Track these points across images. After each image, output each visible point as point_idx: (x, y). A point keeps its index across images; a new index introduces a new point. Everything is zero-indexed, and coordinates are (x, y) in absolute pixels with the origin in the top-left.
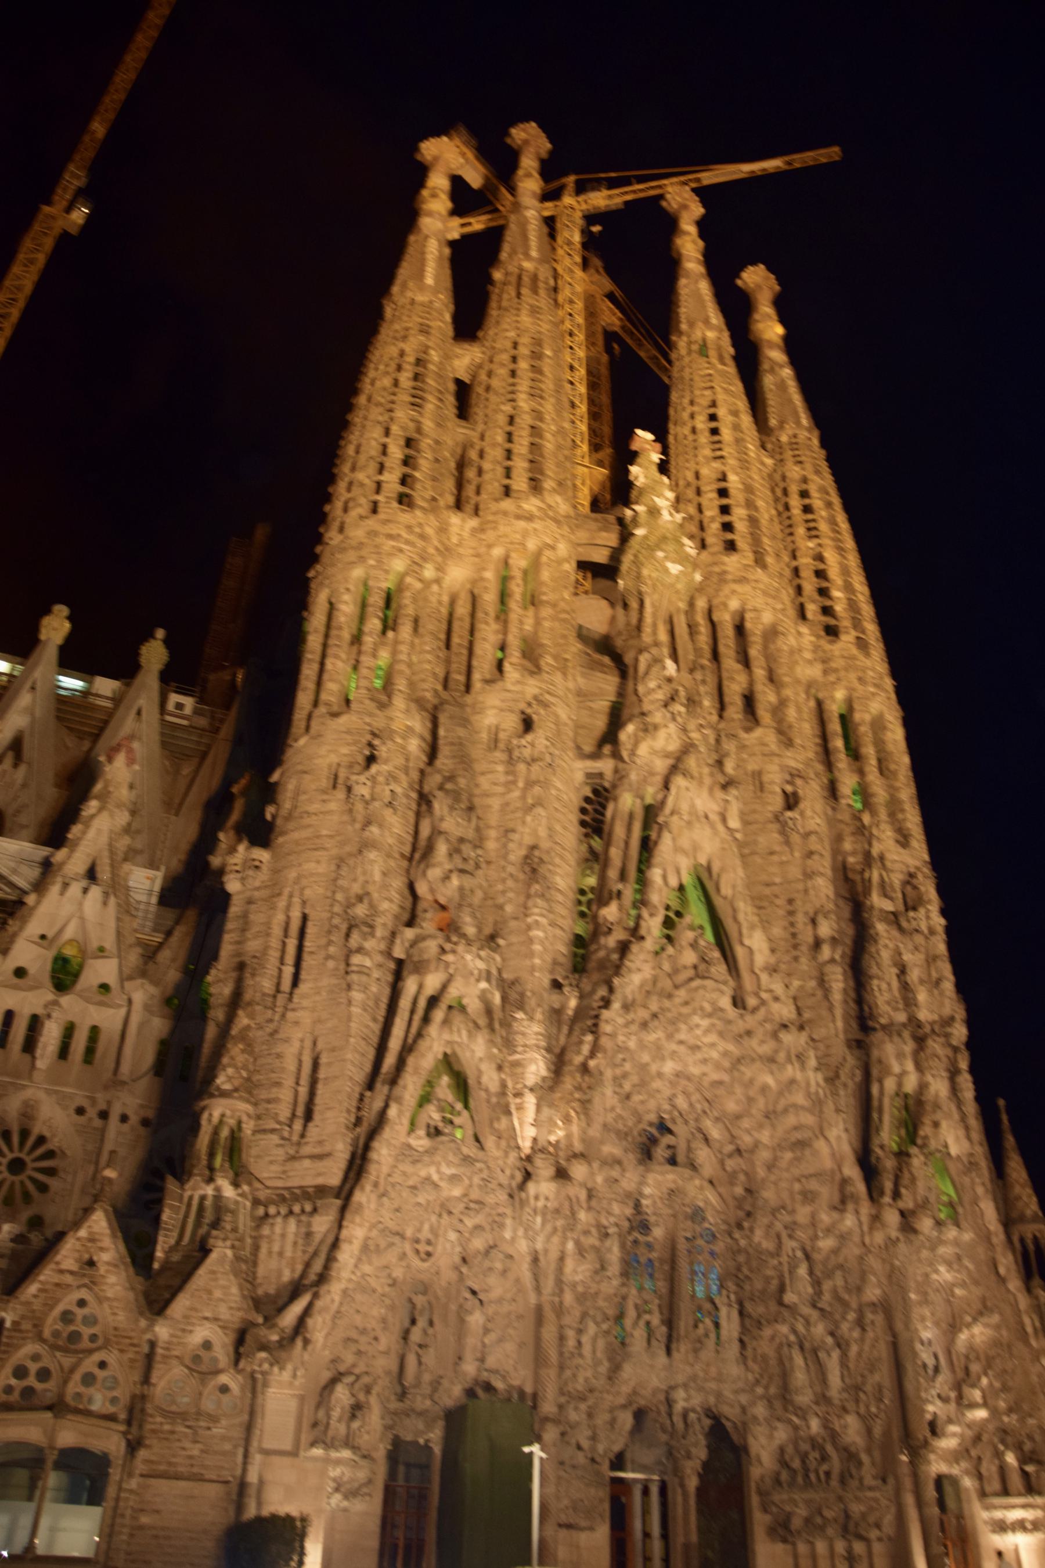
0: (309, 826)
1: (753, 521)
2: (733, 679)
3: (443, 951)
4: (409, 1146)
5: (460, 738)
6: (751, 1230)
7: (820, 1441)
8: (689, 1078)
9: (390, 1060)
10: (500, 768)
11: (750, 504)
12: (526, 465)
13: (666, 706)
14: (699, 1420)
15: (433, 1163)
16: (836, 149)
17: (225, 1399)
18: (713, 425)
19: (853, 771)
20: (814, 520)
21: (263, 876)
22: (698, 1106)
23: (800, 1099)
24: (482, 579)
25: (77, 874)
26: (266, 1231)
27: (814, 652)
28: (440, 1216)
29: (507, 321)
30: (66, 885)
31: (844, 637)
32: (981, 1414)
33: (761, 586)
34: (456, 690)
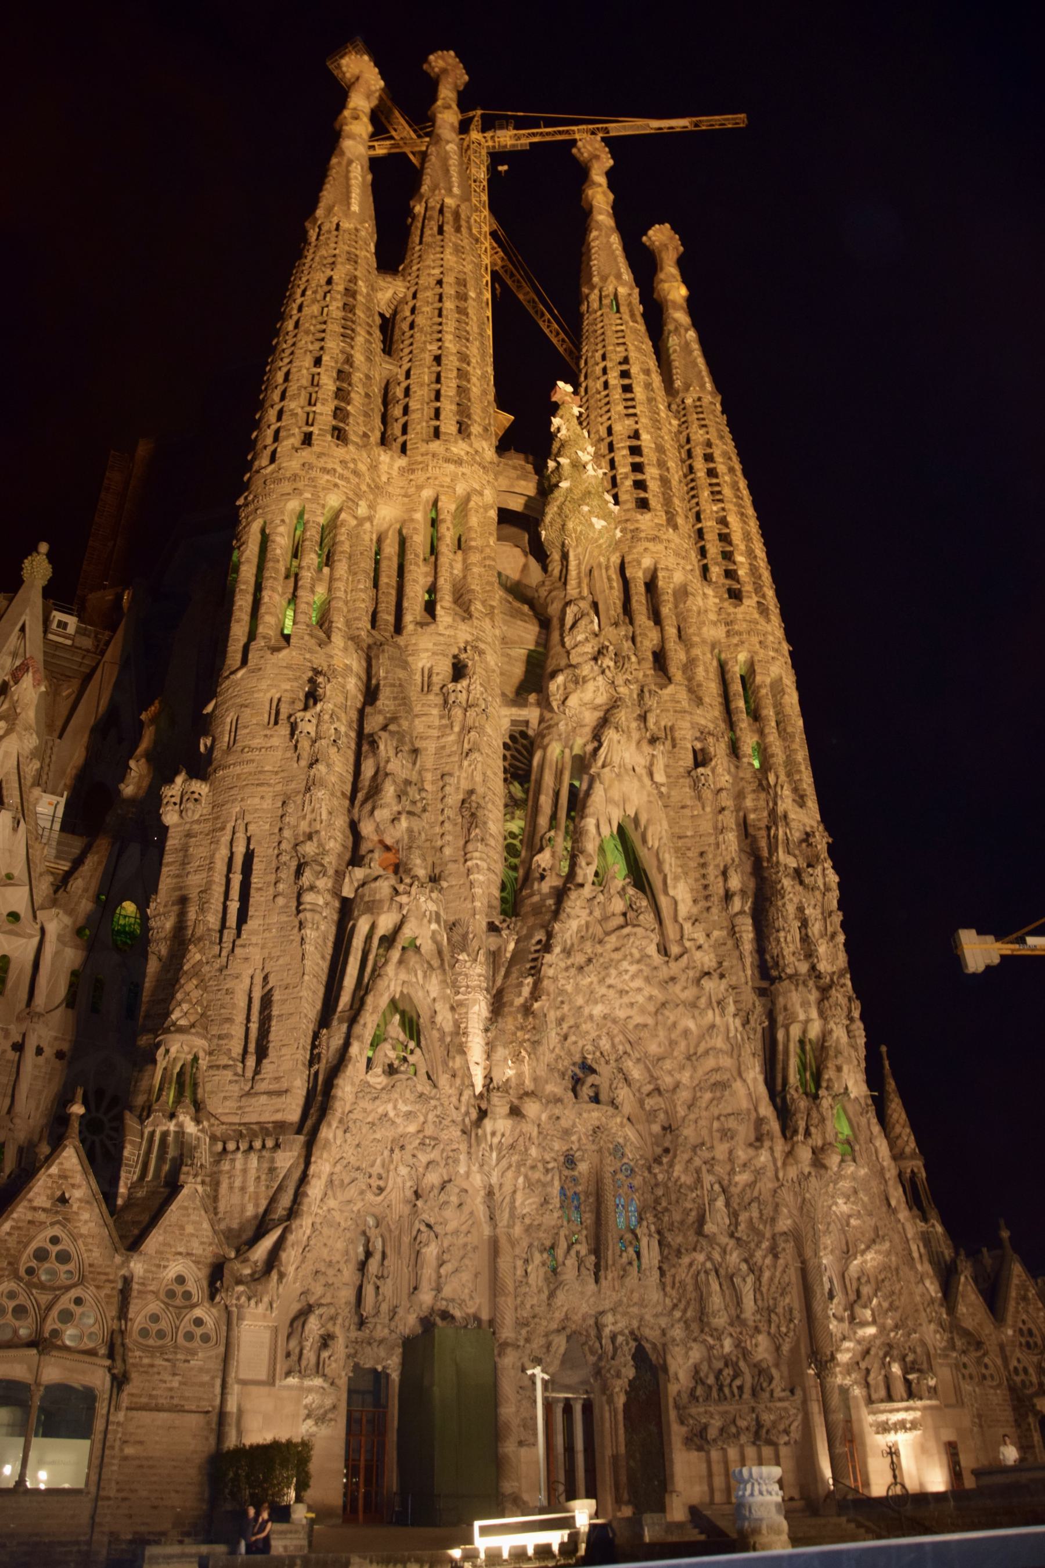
0: (253, 761)
1: (665, 482)
3: (396, 892)
6: (671, 1165)
8: (615, 1021)
9: (345, 998)
10: (435, 712)
11: (661, 464)
12: (454, 407)
13: (595, 659)
16: (743, 116)
18: (626, 382)
19: (752, 731)
20: (718, 484)
21: (203, 809)
22: (621, 1048)
23: (719, 1042)
24: (412, 520)
26: (226, 1166)
28: (392, 1151)
29: (430, 259)
31: (746, 602)
33: (673, 546)
34: (386, 630)
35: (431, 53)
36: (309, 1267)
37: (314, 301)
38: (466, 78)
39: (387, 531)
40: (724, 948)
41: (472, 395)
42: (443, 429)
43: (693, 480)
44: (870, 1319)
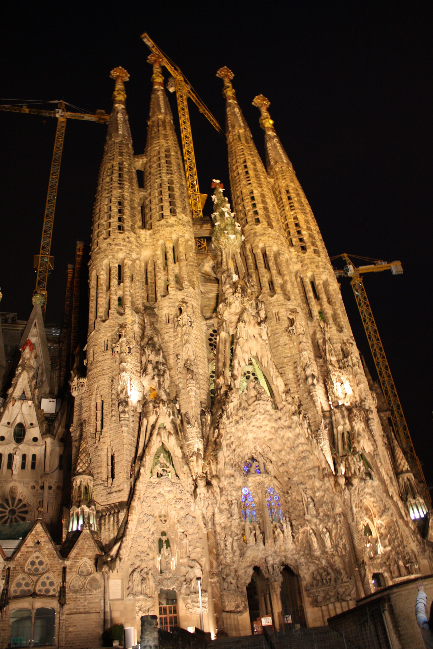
1: (266, 209)
2: (264, 276)
4: (151, 482)
7: (326, 568)
9: (140, 451)
10: (172, 330)
11: (264, 202)
13: (233, 294)
14: (278, 567)
15: (160, 487)
18: (246, 170)
19: (318, 305)
20: (292, 203)
24: (156, 254)
27: (297, 258)
33: (271, 235)
34: (152, 301)
36: (133, 554)
39: (148, 261)
40: (307, 400)
42: (164, 214)
44: (388, 544)
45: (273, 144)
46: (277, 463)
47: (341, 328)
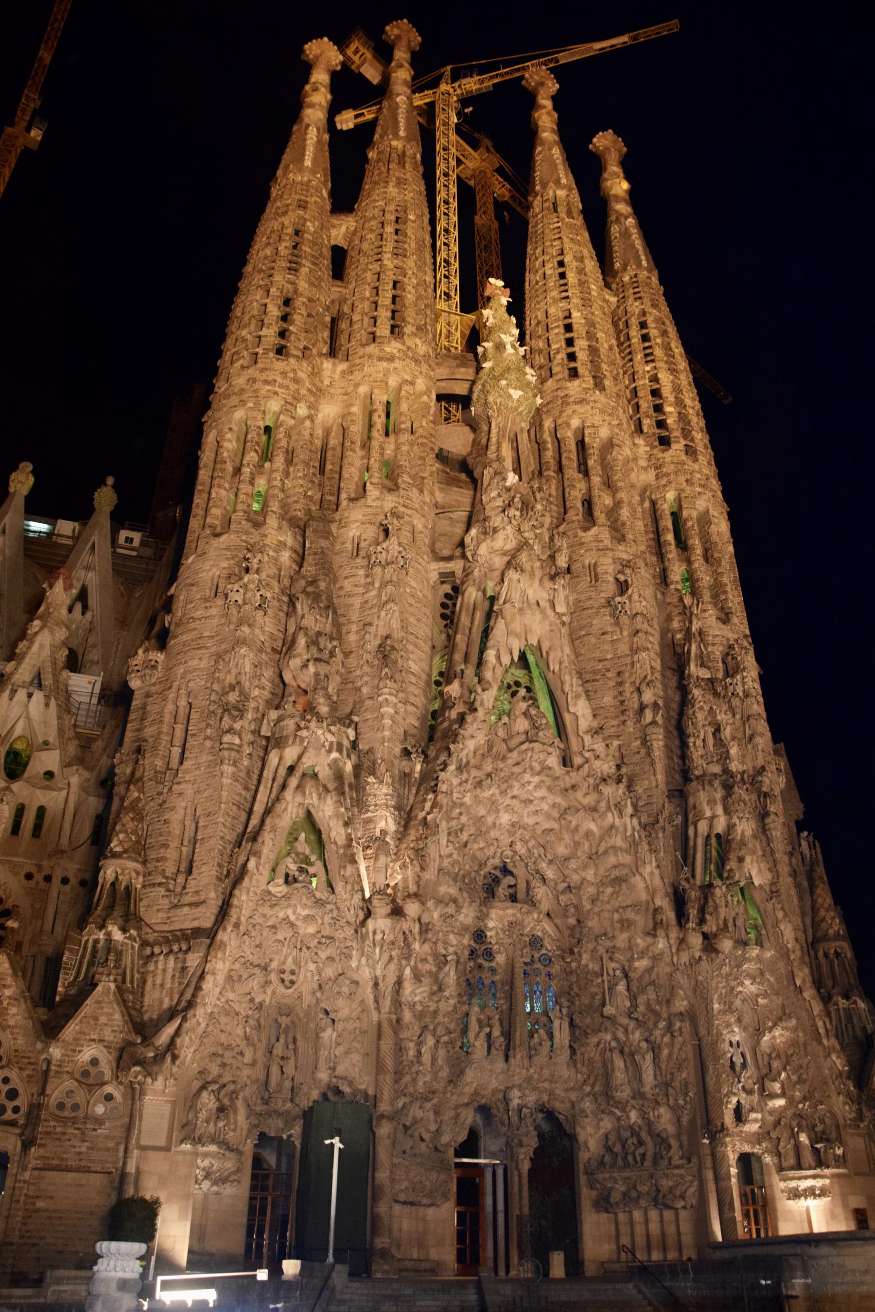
0: (195, 629)
1: (593, 351)
2: (574, 486)
3: (299, 728)
4: (269, 893)
5: (322, 548)
7: (637, 1129)
8: (524, 827)
9: (255, 821)
10: (361, 572)
14: (532, 1115)
15: (289, 906)
17: (111, 1104)
19: (681, 560)
20: (650, 347)
21: (159, 673)
22: (535, 851)
23: (619, 842)
24: (350, 414)
25: (24, 682)
26: (151, 967)
30: (14, 692)
31: (674, 446)
32: (780, 1102)
33: (599, 405)
34: (329, 509)
35: (388, 24)
37: (268, 244)
38: (420, 39)
40: (637, 756)
41: (406, 301)
42: (378, 334)
43: (629, 346)
44: (779, 1092)
45: (623, 229)
46: (556, 884)
47: (727, 614)
